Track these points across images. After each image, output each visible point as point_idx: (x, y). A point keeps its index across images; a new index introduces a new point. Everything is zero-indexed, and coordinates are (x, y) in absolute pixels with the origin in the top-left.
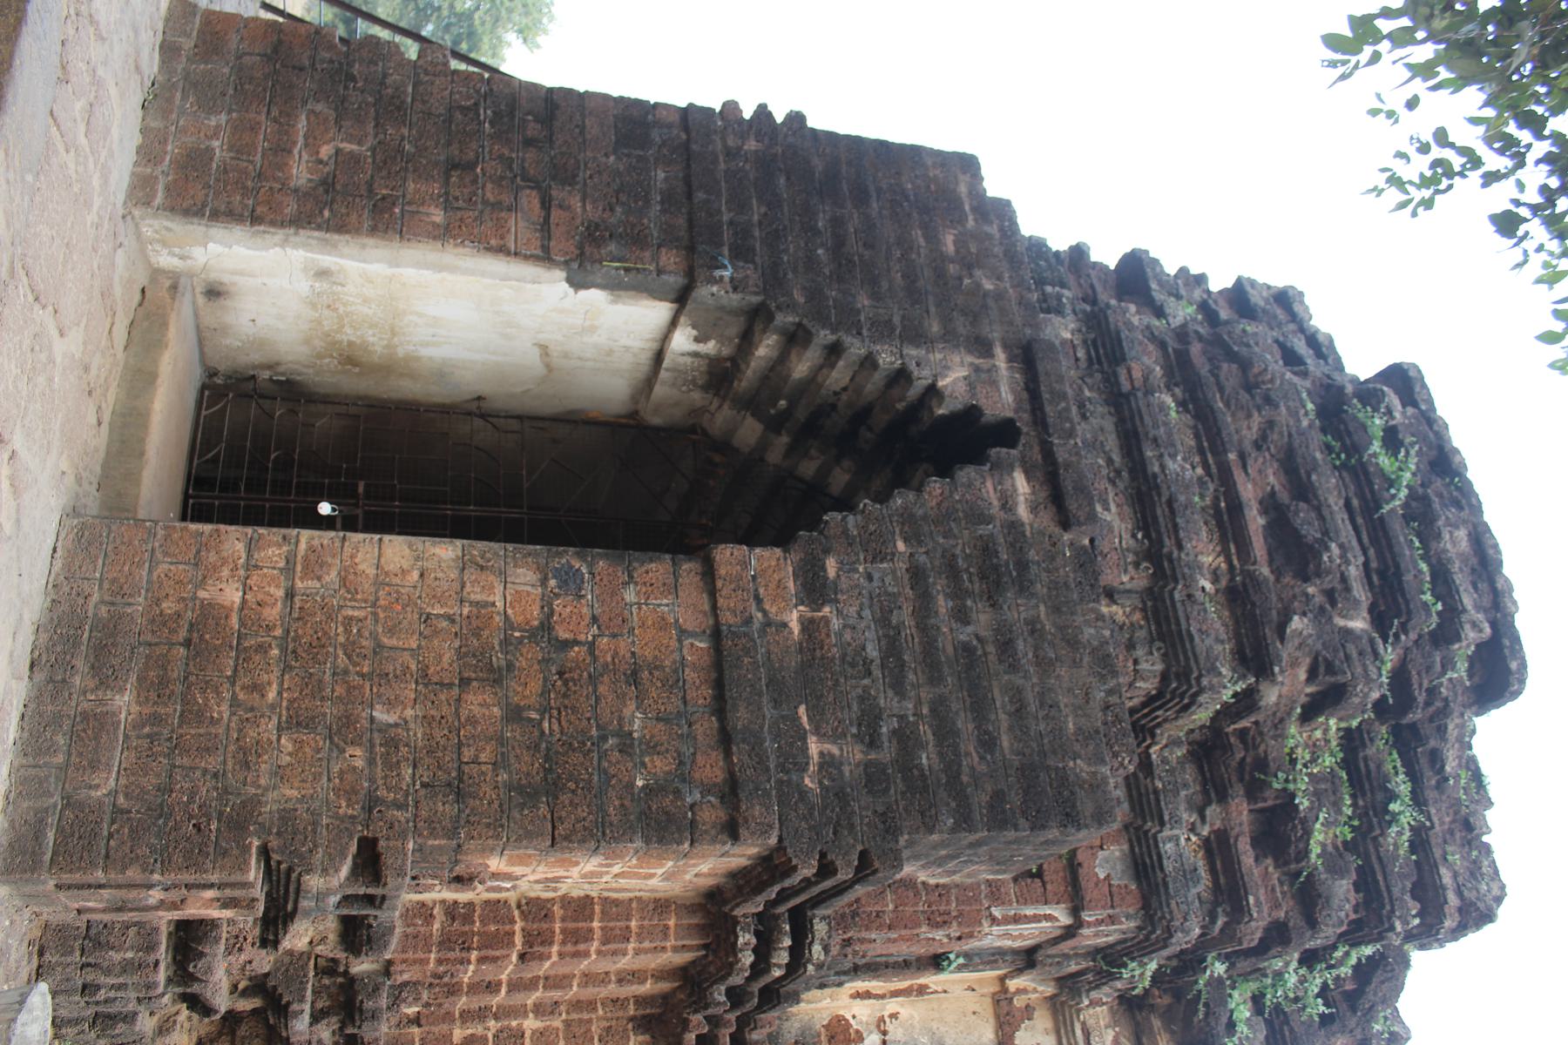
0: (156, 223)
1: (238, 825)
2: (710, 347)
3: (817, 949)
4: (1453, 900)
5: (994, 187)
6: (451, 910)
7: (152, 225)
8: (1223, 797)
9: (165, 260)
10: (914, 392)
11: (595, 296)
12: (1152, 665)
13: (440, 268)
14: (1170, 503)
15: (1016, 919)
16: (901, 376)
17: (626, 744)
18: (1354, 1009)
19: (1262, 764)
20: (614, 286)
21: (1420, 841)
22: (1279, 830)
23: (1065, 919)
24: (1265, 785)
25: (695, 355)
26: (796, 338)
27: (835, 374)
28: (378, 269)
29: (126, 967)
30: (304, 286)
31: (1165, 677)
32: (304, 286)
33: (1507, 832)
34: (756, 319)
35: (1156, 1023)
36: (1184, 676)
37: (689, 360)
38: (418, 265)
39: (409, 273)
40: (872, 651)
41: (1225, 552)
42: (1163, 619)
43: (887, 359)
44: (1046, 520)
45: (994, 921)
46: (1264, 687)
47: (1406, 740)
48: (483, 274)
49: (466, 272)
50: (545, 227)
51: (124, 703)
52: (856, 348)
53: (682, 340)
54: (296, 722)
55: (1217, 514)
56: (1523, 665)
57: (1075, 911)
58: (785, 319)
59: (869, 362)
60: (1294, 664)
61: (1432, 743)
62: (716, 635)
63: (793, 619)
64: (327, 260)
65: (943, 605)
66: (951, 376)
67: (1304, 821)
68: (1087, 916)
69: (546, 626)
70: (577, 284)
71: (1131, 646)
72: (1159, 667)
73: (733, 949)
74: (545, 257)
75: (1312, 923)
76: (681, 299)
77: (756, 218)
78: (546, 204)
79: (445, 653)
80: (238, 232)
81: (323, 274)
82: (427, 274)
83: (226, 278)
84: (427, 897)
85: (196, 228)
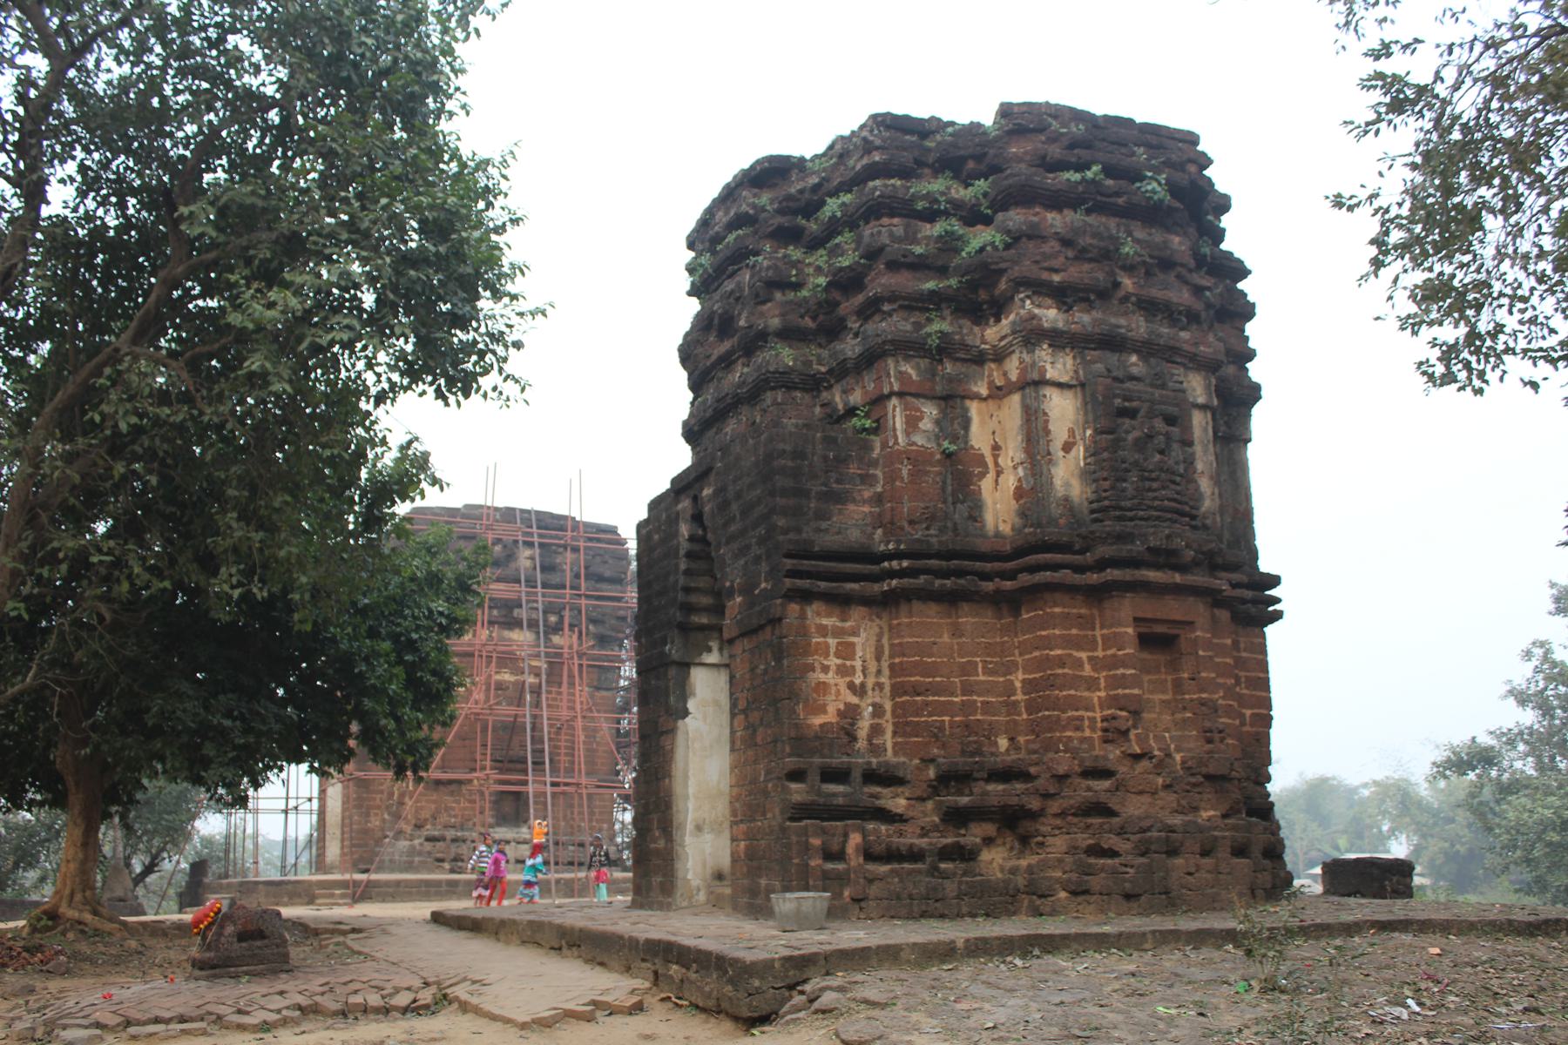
0: (679, 900)
1: (783, 830)
2: (714, 645)
3: (891, 546)
4: (865, 161)
5: (644, 515)
6: (895, 733)
7: (679, 899)
8: (843, 320)
9: (702, 897)
10: (696, 547)
11: (691, 705)
12: (769, 396)
13: (686, 777)
14: (718, 401)
15: (894, 430)
16: (689, 555)
17: (766, 671)
18: (985, 154)
19: (819, 304)
20: (684, 696)
21: (846, 187)
22: (848, 282)
23: (894, 401)
24: (826, 301)
25: (721, 650)
26: (689, 609)
27: (701, 585)
28: (691, 806)
29: (901, 881)
30: (708, 837)
31: (773, 389)
32: (708, 837)
33: (849, 122)
34: (685, 629)
35: (997, 292)
36: (767, 381)
37: (725, 653)
38: (686, 786)
39: (691, 791)
40: (742, 562)
41: (735, 362)
42: (752, 395)
43: (683, 566)
44: (712, 478)
45: (896, 443)
46: (770, 330)
47: (811, 209)
48: (687, 756)
49: (687, 764)
50: (667, 732)
51: (763, 882)
52: (682, 581)
53: (713, 658)
54: (764, 814)
55: (728, 366)
56: (758, 162)
57: (889, 396)
58: (679, 616)
59: (688, 572)
60: (762, 314)
61: (807, 195)
62: (743, 635)
63: (739, 600)
64: (689, 827)
65: (733, 528)
66: (684, 530)
67: (834, 275)
68: (886, 391)
69: (744, 711)
70: (686, 713)
71: (765, 411)
72: (769, 394)
73: (892, 591)
74: (672, 731)
75: (881, 249)
76: (685, 666)
77: (513, 678)
78: (663, 733)
79: (750, 753)
80: (678, 865)
81: (699, 828)
82: (692, 782)
83: (709, 871)
84: (889, 745)
85: (679, 883)
